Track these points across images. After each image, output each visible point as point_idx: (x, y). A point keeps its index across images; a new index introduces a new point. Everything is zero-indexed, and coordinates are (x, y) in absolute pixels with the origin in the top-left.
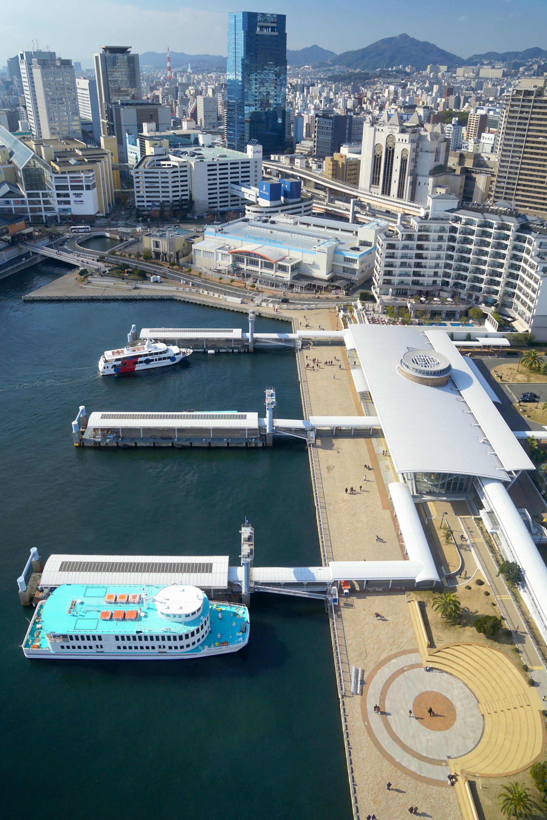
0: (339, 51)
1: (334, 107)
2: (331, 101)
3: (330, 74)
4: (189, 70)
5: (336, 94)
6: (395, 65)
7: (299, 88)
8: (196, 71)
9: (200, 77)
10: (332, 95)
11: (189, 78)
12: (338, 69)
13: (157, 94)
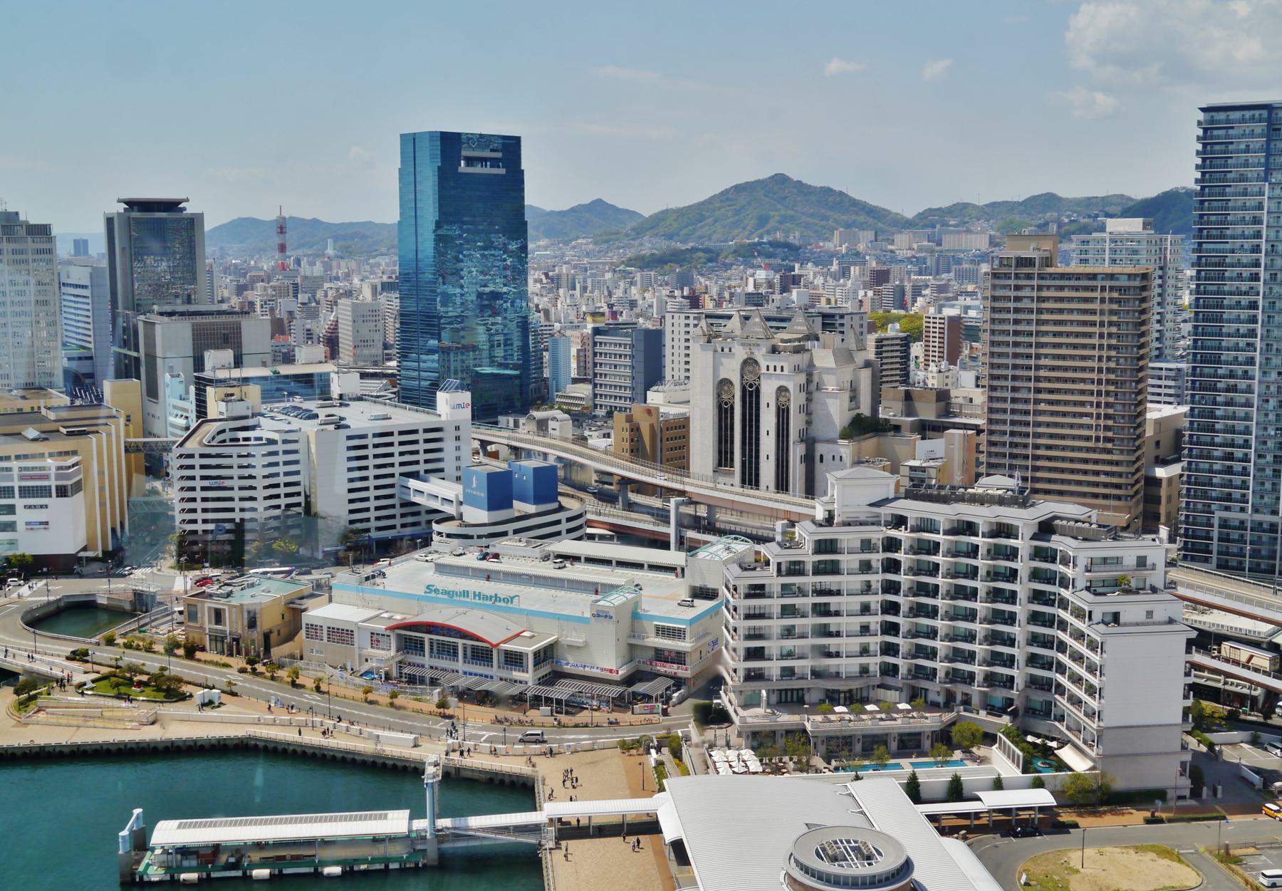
1: (638, 316)
2: (633, 304)
3: (630, 253)
5: (644, 290)
6: (768, 232)
7: (564, 282)
8: (346, 253)
9: (353, 265)
10: (634, 292)
11: (327, 267)
12: (649, 246)
13: (250, 299)
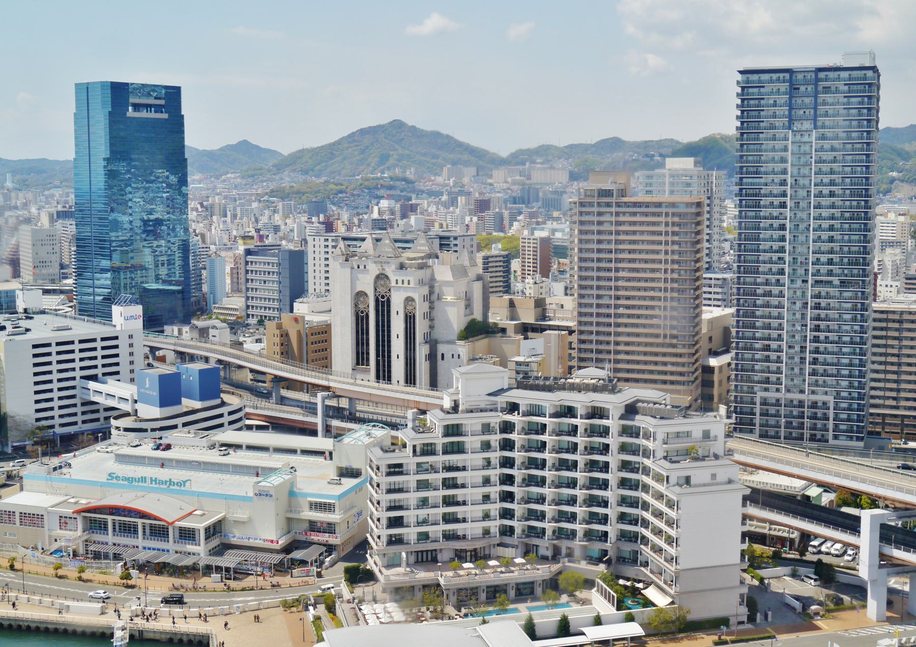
0: (286, 149)
1: (281, 239)
2: (276, 229)
3: (272, 186)
4: (9, 184)
5: (286, 217)
6: (389, 168)
7: (217, 210)
8: (23, 185)
9: (30, 196)
10: (278, 219)
12: (287, 180)
